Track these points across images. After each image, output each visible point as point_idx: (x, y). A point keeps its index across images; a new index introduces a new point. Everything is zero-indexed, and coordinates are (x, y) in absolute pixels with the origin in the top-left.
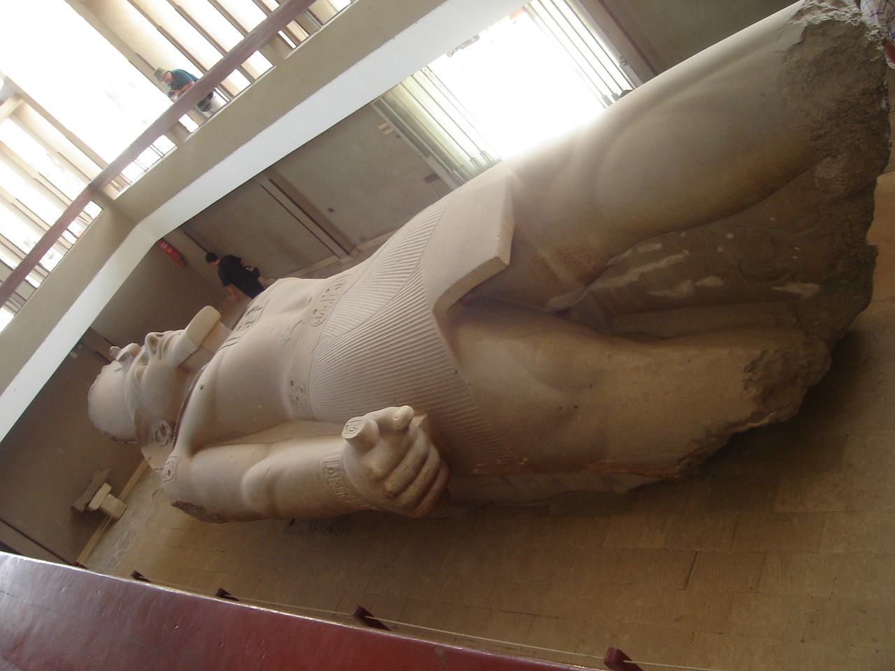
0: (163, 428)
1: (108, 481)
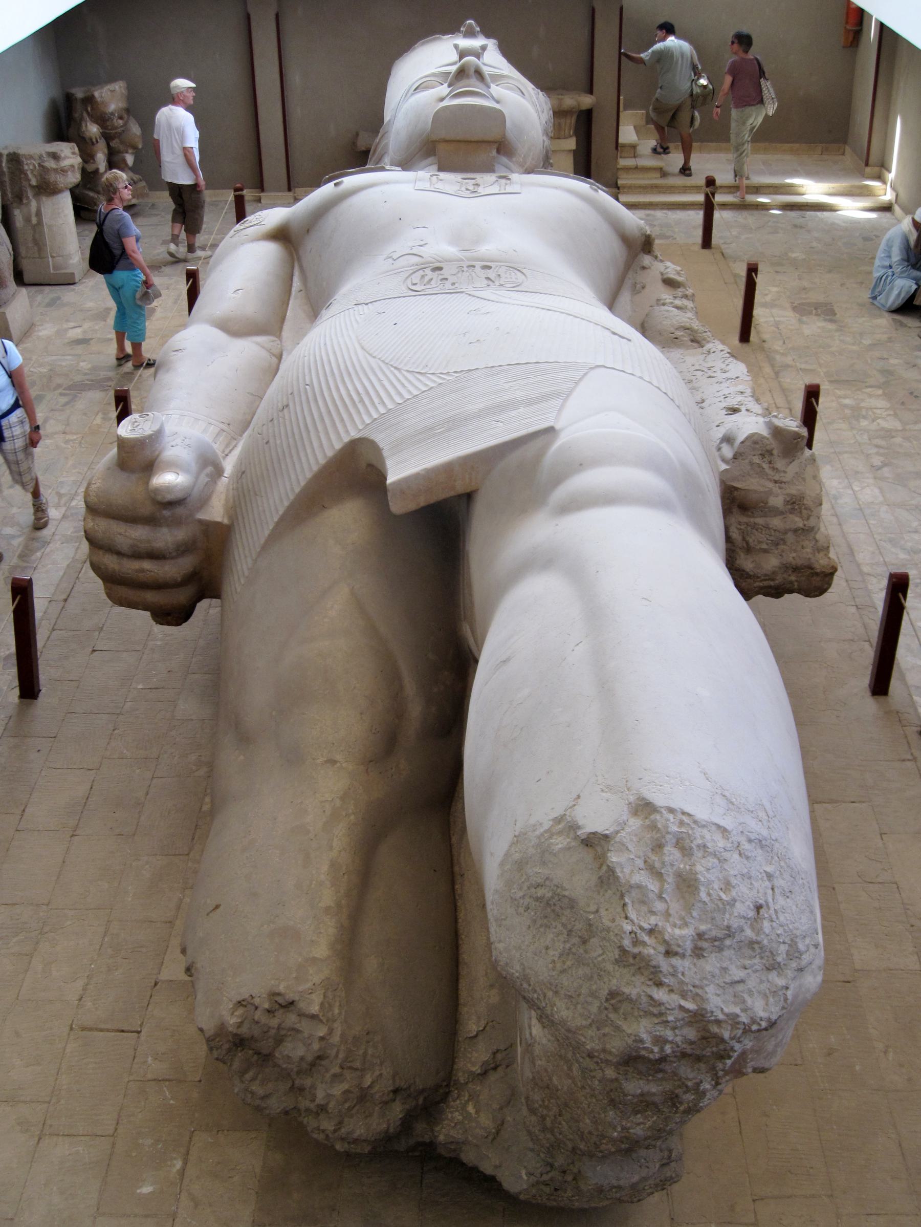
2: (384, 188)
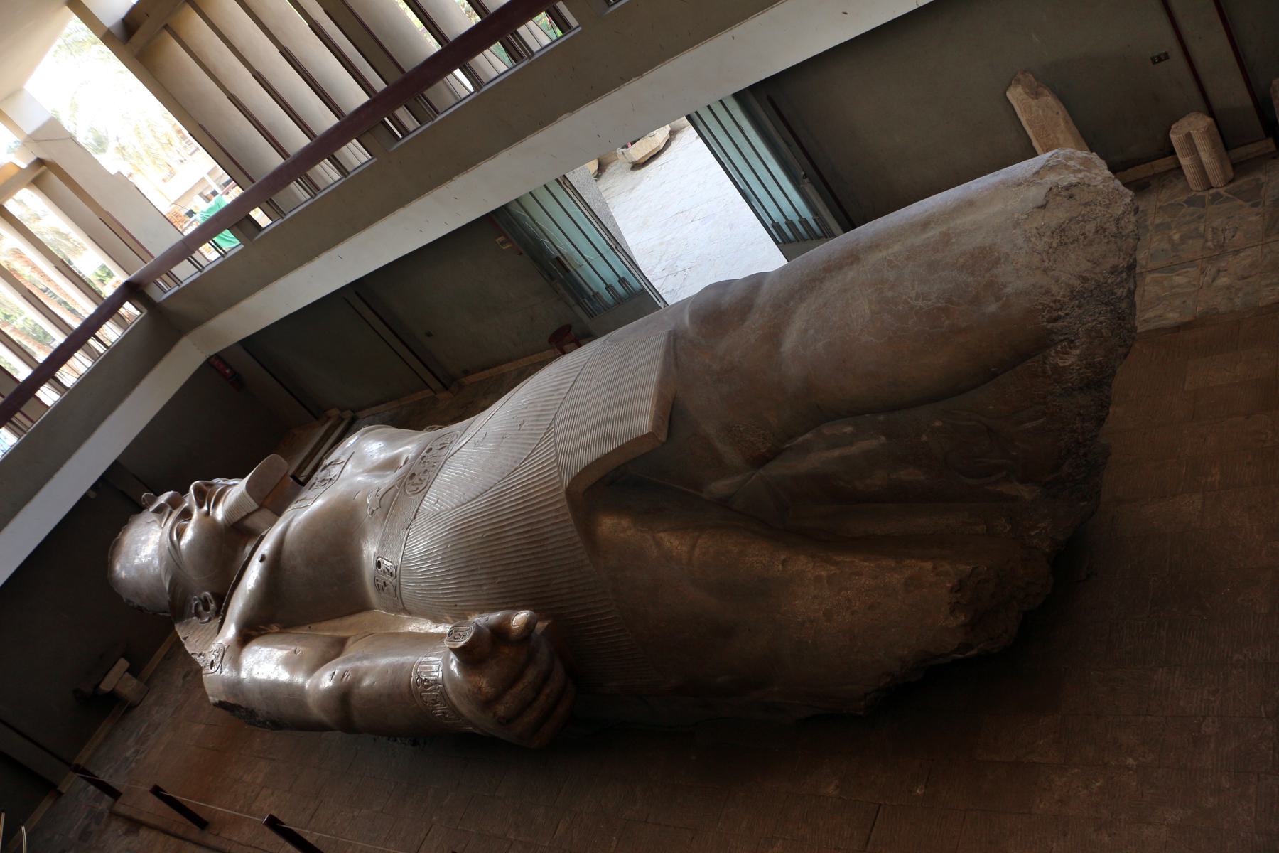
0: (205, 602)
1: (125, 656)
2: (294, 524)
